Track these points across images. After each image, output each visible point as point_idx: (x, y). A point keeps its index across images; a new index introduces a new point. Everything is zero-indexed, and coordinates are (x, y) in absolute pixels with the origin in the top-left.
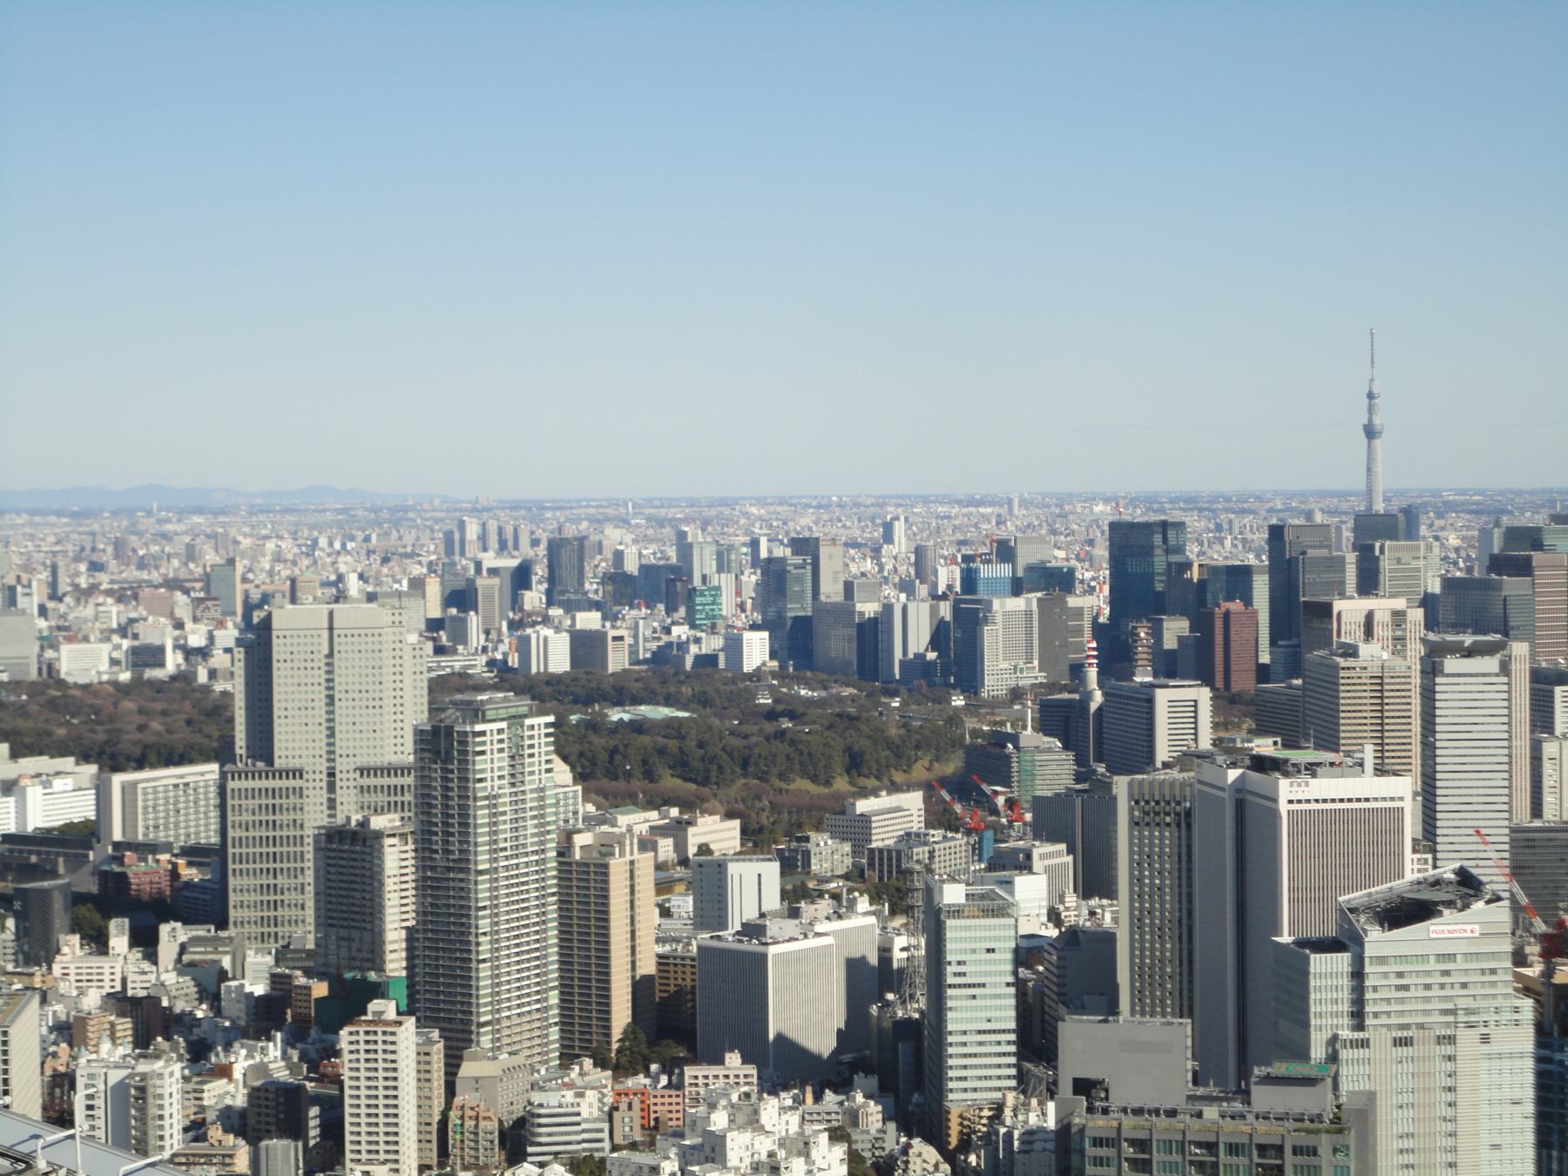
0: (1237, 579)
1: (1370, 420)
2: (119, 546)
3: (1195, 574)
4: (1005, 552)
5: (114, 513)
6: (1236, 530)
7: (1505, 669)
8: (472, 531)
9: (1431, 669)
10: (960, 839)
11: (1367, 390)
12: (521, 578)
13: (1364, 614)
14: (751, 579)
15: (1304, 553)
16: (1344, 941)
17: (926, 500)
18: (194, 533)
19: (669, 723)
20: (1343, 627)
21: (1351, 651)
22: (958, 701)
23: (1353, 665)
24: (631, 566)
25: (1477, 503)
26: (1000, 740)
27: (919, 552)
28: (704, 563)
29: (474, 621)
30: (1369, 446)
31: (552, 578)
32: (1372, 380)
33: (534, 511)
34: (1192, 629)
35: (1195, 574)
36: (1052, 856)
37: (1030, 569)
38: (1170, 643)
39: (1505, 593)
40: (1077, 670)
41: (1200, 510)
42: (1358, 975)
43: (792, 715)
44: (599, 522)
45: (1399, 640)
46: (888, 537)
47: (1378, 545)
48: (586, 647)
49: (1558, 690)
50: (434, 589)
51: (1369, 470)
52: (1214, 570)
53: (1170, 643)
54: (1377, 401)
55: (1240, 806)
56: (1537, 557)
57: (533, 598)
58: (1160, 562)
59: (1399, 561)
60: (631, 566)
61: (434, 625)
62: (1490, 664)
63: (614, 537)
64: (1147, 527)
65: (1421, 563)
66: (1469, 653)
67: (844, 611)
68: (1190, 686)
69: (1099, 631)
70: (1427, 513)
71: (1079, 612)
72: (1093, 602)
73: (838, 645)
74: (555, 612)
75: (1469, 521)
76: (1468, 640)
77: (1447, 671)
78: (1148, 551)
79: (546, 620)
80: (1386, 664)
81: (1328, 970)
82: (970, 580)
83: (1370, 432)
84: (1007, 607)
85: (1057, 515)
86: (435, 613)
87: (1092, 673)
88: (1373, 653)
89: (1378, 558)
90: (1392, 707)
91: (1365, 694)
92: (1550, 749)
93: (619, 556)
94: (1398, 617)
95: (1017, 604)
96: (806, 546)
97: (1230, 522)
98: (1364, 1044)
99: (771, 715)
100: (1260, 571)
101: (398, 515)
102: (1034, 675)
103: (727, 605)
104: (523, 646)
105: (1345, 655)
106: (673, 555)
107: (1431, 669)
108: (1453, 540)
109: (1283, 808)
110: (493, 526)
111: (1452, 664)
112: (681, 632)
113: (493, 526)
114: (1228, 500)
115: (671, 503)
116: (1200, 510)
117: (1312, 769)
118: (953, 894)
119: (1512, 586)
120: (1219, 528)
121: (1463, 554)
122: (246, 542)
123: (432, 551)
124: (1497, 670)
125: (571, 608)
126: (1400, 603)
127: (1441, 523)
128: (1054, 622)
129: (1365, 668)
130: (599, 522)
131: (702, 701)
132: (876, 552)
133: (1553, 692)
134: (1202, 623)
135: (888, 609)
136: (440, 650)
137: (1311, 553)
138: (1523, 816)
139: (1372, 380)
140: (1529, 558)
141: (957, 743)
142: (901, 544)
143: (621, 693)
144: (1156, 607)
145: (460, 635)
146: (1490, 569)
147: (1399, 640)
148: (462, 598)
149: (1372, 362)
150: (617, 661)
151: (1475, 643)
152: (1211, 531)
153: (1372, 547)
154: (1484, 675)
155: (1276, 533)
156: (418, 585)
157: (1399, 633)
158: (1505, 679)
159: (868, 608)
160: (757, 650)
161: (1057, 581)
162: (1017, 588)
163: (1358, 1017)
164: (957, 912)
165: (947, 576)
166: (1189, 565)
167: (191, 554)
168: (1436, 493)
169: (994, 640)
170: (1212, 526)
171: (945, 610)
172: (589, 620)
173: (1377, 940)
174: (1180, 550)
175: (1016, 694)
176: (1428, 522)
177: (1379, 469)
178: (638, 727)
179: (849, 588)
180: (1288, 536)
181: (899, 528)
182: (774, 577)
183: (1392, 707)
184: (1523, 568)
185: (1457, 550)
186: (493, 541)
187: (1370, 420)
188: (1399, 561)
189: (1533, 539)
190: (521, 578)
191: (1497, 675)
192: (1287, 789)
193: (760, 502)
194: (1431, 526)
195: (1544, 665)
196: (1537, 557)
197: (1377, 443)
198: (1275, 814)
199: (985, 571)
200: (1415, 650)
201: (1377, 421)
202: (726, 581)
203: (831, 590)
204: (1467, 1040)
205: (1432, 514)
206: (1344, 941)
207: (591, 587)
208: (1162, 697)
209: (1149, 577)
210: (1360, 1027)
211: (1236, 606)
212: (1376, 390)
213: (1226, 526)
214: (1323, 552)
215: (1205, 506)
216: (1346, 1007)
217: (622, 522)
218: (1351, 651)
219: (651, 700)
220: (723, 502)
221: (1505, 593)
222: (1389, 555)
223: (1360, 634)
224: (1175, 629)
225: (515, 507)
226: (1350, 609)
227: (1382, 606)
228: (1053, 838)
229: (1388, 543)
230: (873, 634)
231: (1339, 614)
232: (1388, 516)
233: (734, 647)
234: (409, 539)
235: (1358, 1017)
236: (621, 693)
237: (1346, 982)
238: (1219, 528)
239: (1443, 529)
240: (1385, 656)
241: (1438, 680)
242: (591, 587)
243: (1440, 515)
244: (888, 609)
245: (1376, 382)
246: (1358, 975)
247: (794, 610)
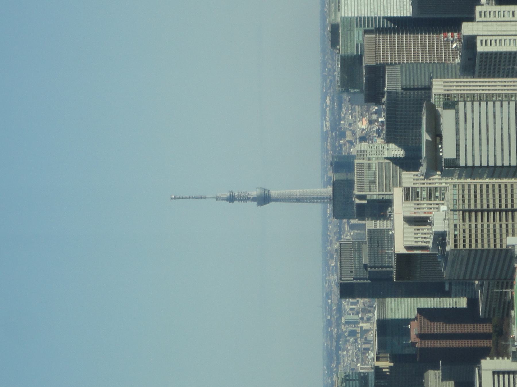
1: (254, 199)
3: (385, 365)
6: (355, 317)
11: (226, 203)
13: (407, 226)
15: (365, 266)
20: (420, 244)
23: (452, 237)
25: (332, 101)
30: (277, 200)
32: (217, 198)
34: (435, 367)
35: (385, 365)
39: (399, 90)
41: (338, 348)
47: (357, 201)
49: (480, 49)
51: (299, 200)
52: (382, 347)
54: (236, 194)
56: (367, 61)
59: (373, 182)
65: (374, 162)
68: (480, 378)
70: (341, 146)
75: (347, 109)
76: (426, 137)
77: (454, 157)
80: (452, 207)
89: (368, 201)
90: (491, 201)
91: (479, 226)
97: (347, 323)
100: (382, 309)
105: (444, 244)
108: (363, 125)
114: (329, 323)
116: (338, 348)
120: (352, 333)
121: (374, 117)
124: (453, 112)
126: (398, 194)
127: (348, 133)
129: (455, 226)
133: (482, 54)
137: (365, 260)
139: (217, 198)
140: (368, 67)
146: (378, 102)
149: (201, 198)
151: (428, 131)
152: (356, 341)
153: (359, 206)
154: (457, 123)
157: (425, 194)
158: (461, 105)
166: (378, 370)
168: (325, 137)
170: (352, 339)
176: (348, 145)
177: (297, 192)
180: (349, 279)
183: (491, 201)
185: (371, 122)
187: (254, 199)
188: (373, 182)
191: (457, 112)
194: (351, 143)
195: (458, 60)
196: (367, 61)
197: (274, 193)
201: (254, 193)
205: (342, 142)
211: (414, 329)
212: (227, 194)
213: (351, 328)
214: (365, 249)
215: (334, 344)
221: (399, 90)
223: (425, 229)
229: (356, 192)
231: (408, 248)
232: (336, 185)
238: (352, 333)
239: (354, 133)
240: (444, 208)
241: (462, 163)
243: (342, 135)
245: (219, 194)
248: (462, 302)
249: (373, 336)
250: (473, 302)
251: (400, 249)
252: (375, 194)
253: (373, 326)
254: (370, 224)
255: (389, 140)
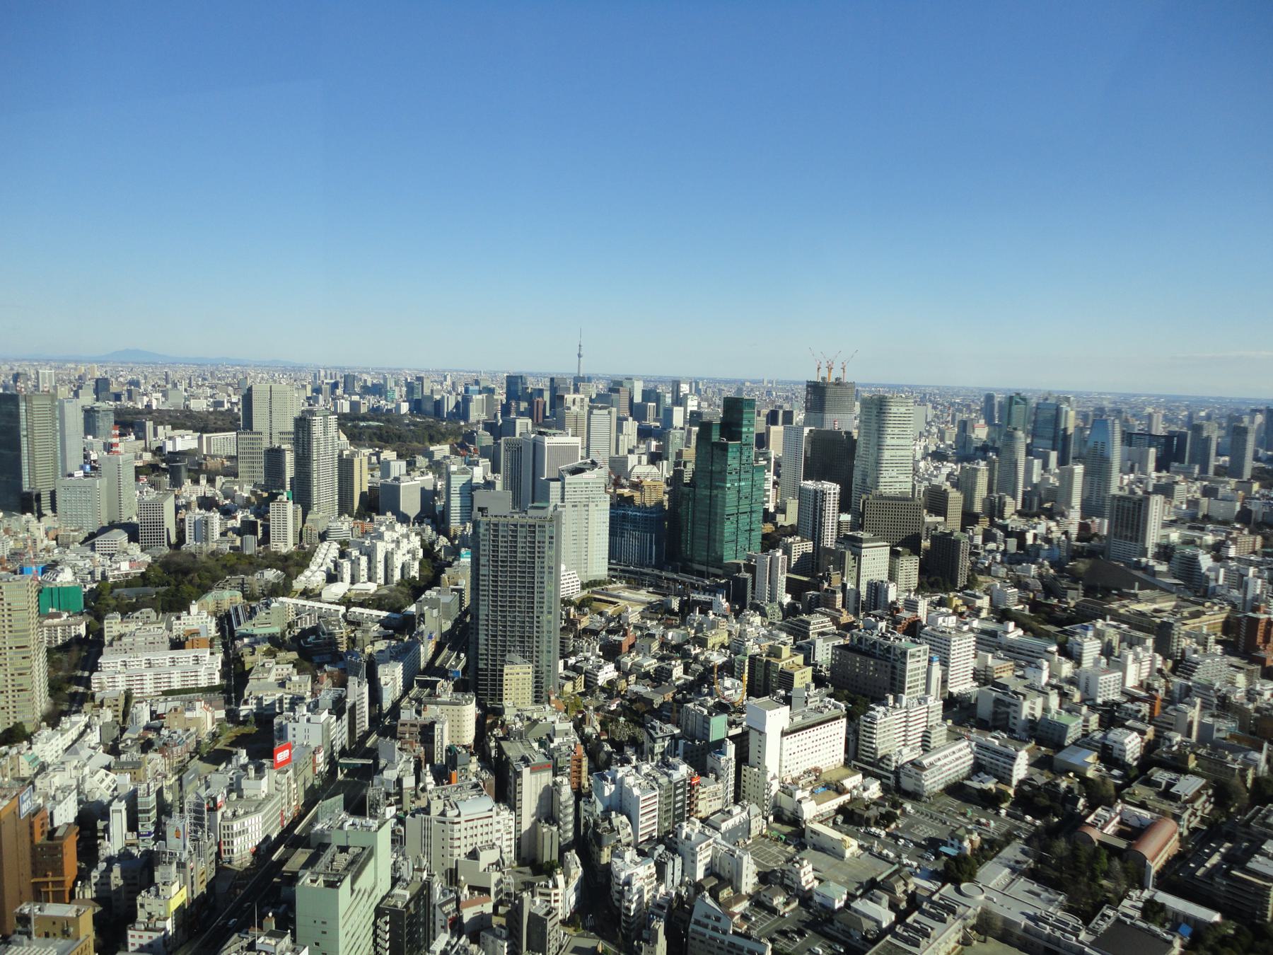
0: (540, 392)
2: (212, 373)
3: (529, 391)
4: (477, 382)
5: (212, 365)
7: (610, 413)
8: (322, 373)
9: (590, 413)
10: (459, 458)
12: (335, 386)
14: (404, 389)
16: (560, 479)
17: (457, 371)
18: (236, 371)
19: (377, 426)
21: (569, 408)
22: (462, 423)
24: (369, 384)
26: (473, 432)
27: (453, 383)
28: (391, 384)
29: (321, 397)
31: (345, 386)
33: (342, 369)
35: (529, 391)
36: (485, 462)
37: (484, 388)
38: (522, 409)
40: (496, 416)
42: (563, 488)
43: (414, 425)
44: (361, 373)
45: (582, 406)
46: (445, 380)
48: (354, 406)
50: (309, 388)
53: (522, 409)
55: (534, 445)
57: (339, 391)
58: (520, 387)
60: (369, 384)
61: (308, 398)
62: (605, 412)
63: (365, 376)
64: (516, 377)
66: (600, 409)
67: (431, 397)
69: (502, 405)
71: (497, 400)
72: (500, 396)
73: (428, 407)
74: (346, 396)
78: (516, 383)
79: (343, 398)
81: (555, 486)
82: (467, 390)
83: (580, 356)
84: (477, 397)
85: (493, 376)
86: (309, 395)
87: (499, 415)
88: (575, 409)
92: (621, 437)
93: (365, 381)
94: (582, 400)
95: (480, 397)
96: (420, 379)
98: (564, 506)
99: (408, 425)
101: (300, 369)
102: (484, 417)
103: (397, 396)
104: (335, 405)
106: (382, 382)
107: (590, 413)
109: (546, 445)
110: (329, 372)
111: (595, 411)
112: (383, 402)
113: (329, 372)
115: (383, 369)
117: (554, 435)
118: (453, 468)
119: (614, 396)
122: (252, 374)
123: (310, 379)
125: (350, 395)
126: (583, 396)
128: (490, 403)
130: (361, 373)
131: (388, 421)
132: (442, 384)
134: (531, 404)
135: (443, 397)
136: (310, 405)
138: (613, 454)
141: (461, 434)
142: (449, 382)
143: (364, 418)
144: (518, 399)
145: (316, 401)
147: (582, 406)
148: (317, 390)
150: (364, 410)
155: (552, 380)
156: (304, 387)
159: (437, 397)
160: (405, 408)
161: (491, 391)
162: (480, 393)
163: (563, 499)
164: (454, 473)
165: (461, 389)
167: (234, 376)
169: (473, 407)
171: (460, 398)
172: (355, 398)
173: (569, 478)
174: (525, 384)
175: (478, 422)
178: (368, 427)
179: (432, 391)
181: (448, 377)
182: (410, 387)
184: (617, 391)
186: (329, 376)
189: (620, 384)
190: (335, 386)
192: (548, 441)
193: (409, 369)
198: (544, 447)
199: (471, 388)
200: (586, 408)
202: (397, 389)
203: (427, 392)
204: (592, 506)
206: (560, 479)
207: (357, 390)
208: (518, 421)
209: (516, 391)
210: (563, 502)
211: (540, 399)
216: (559, 497)
217: (368, 373)
218: (569, 408)
219: (373, 420)
220: (400, 369)
222: (582, 386)
224: (524, 405)
225: (336, 368)
226: (569, 397)
227: (578, 397)
228: (485, 457)
230: (438, 405)
232: (583, 378)
233: (398, 407)
234: (303, 375)
235: (563, 499)
236: (364, 418)
237: (560, 490)
242: (357, 390)
244: (443, 397)
246: (563, 488)
247: (416, 397)
248: (548, 414)
249: (537, 387)
250: (548, 417)
251: (566, 396)
252: (581, 389)
253: (540, 386)
254: (572, 387)
255: (597, 395)
